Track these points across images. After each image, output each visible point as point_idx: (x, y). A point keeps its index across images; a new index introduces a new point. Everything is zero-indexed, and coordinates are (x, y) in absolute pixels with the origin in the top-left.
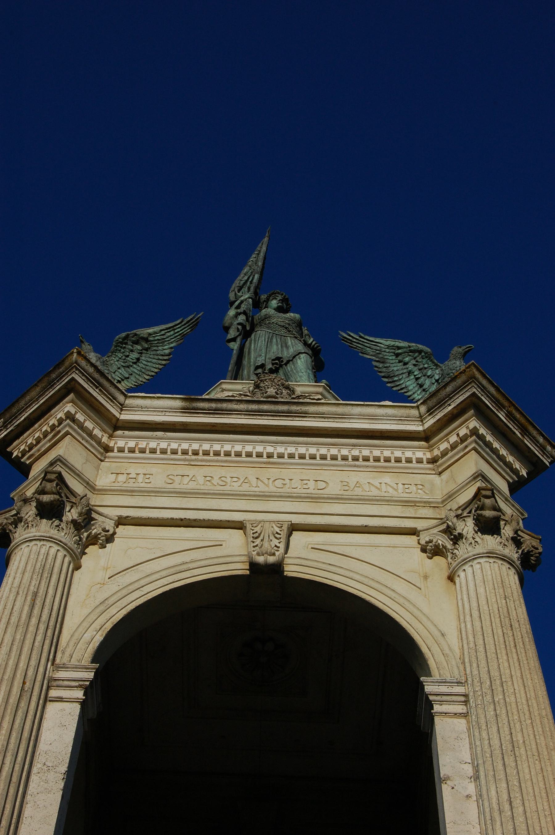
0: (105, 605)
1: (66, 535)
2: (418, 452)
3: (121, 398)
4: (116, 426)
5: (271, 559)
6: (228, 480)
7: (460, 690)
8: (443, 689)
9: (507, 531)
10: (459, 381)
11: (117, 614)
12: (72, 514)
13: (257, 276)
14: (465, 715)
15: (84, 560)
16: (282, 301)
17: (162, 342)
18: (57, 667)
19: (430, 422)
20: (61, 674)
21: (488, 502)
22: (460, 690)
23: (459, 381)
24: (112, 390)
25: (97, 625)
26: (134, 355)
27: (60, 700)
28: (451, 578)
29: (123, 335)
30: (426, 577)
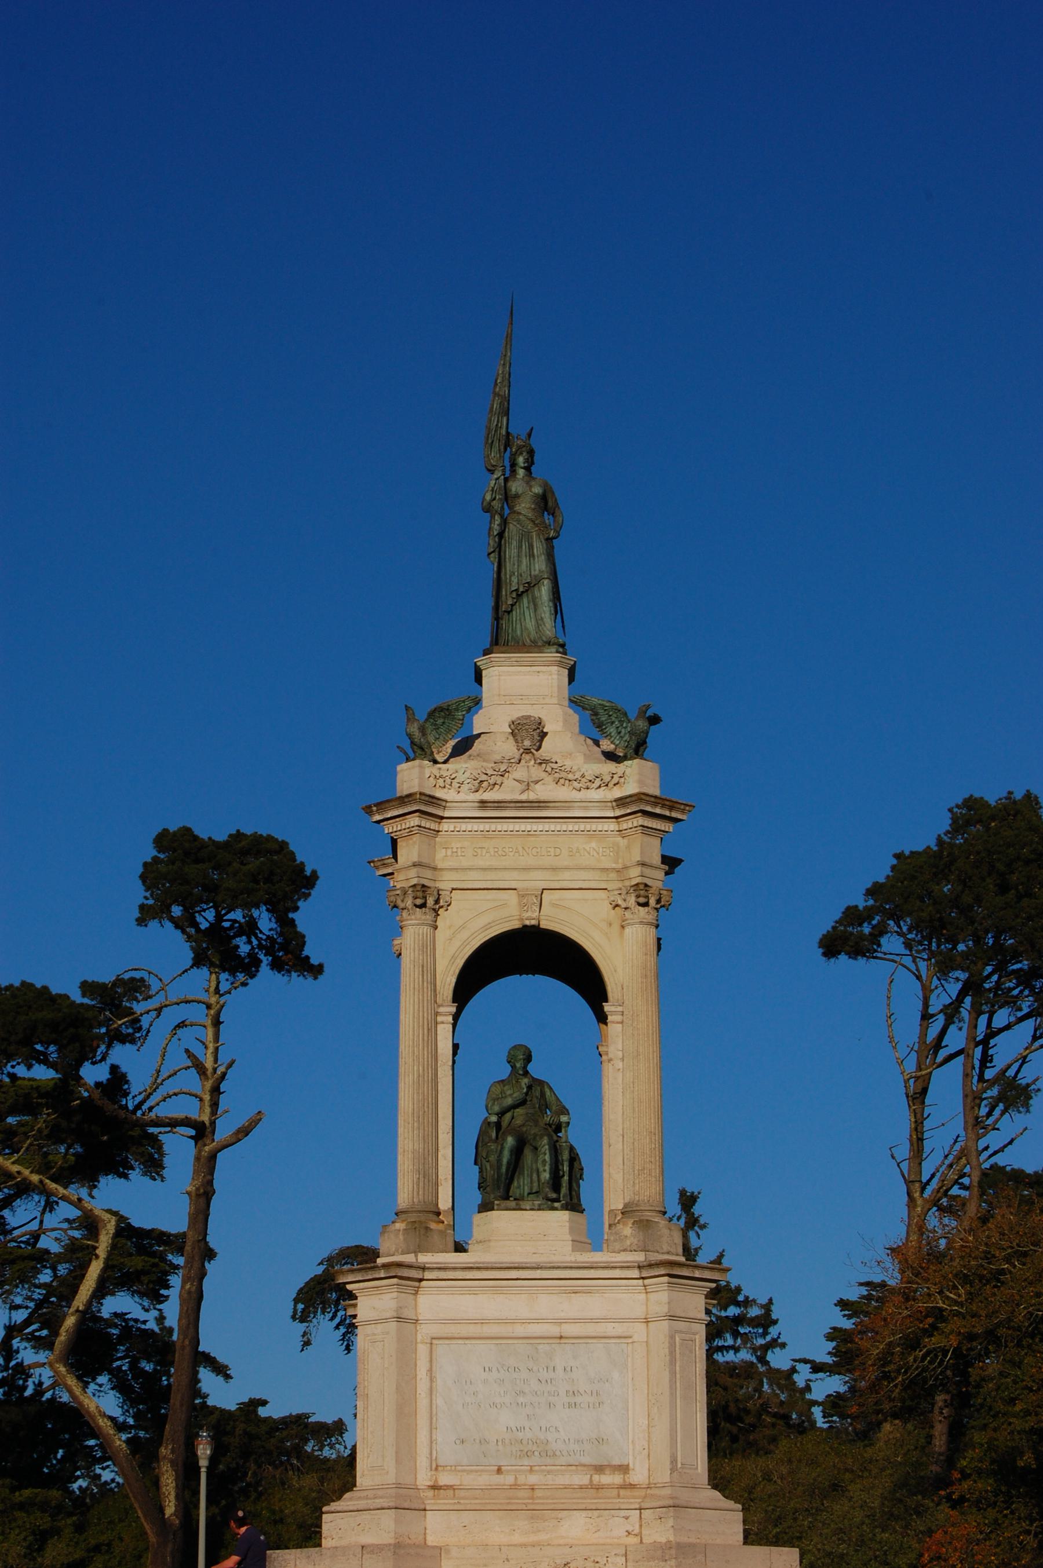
0: (454, 958)
1: (429, 917)
2: (612, 826)
3: (444, 804)
4: (442, 818)
5: (533, 922)
6: (507, 850)
7: (620, 1009)
8: (613, 1009)
9: (652, 902)
10: (633, 799)
11: (460, 963)
12: (430, 902)
13: (505, 419)
14: (622, 1023)
15: (440, 922)
16: (526, 461)
17: (457, 710)
18: (439, 1006)
19: (618, 813)
20: (441, 1010)
21: (642, 892)
22: (620, 1009)
23: (633, 799)
24: (439, 802)
25: (451, 972)
26: (440, 721)
27: (443, 1023)
28: (623, 927)
29: (433, 707)
30: (610, 925)
